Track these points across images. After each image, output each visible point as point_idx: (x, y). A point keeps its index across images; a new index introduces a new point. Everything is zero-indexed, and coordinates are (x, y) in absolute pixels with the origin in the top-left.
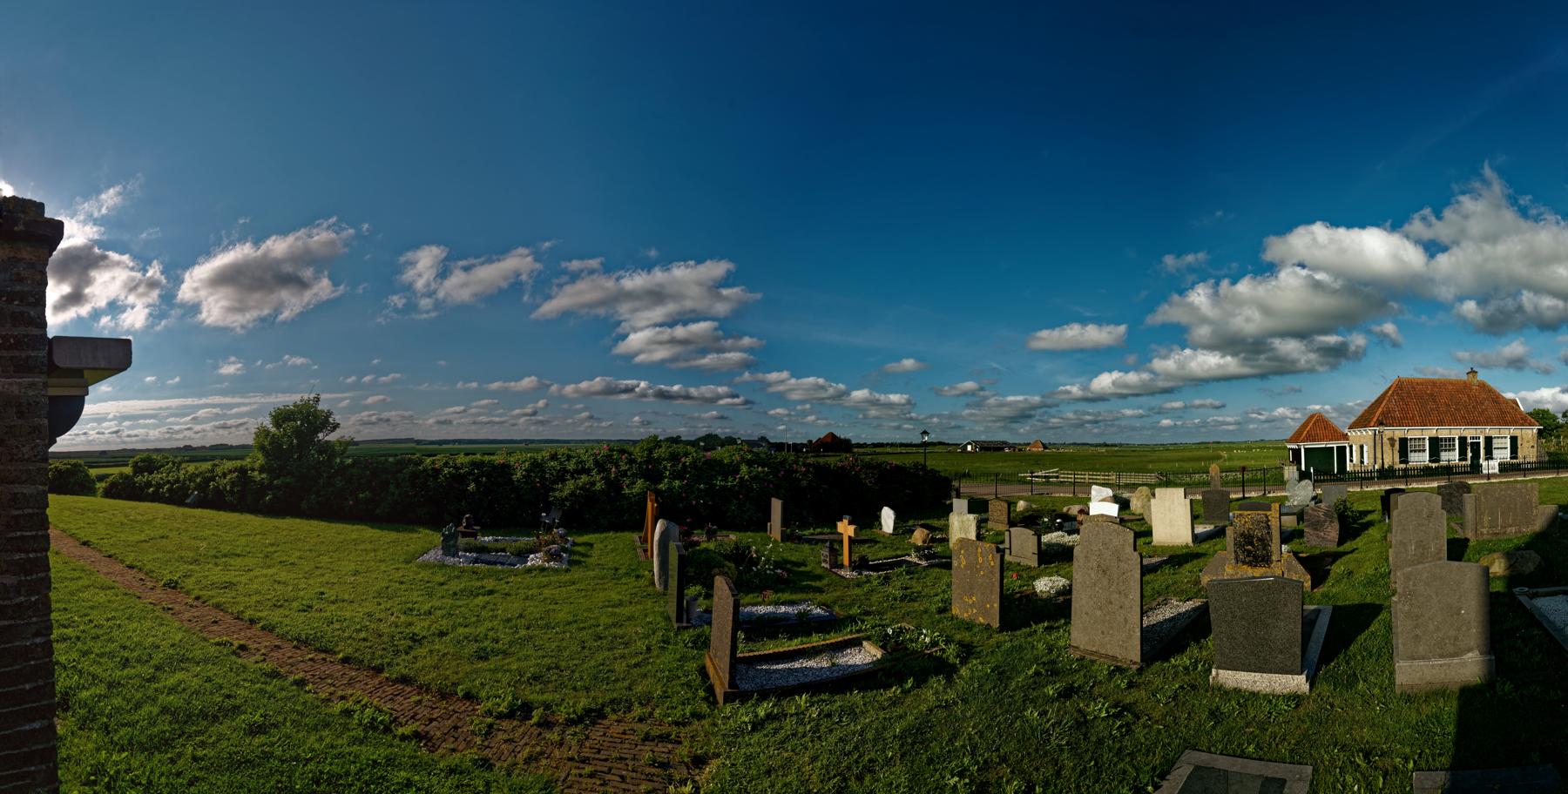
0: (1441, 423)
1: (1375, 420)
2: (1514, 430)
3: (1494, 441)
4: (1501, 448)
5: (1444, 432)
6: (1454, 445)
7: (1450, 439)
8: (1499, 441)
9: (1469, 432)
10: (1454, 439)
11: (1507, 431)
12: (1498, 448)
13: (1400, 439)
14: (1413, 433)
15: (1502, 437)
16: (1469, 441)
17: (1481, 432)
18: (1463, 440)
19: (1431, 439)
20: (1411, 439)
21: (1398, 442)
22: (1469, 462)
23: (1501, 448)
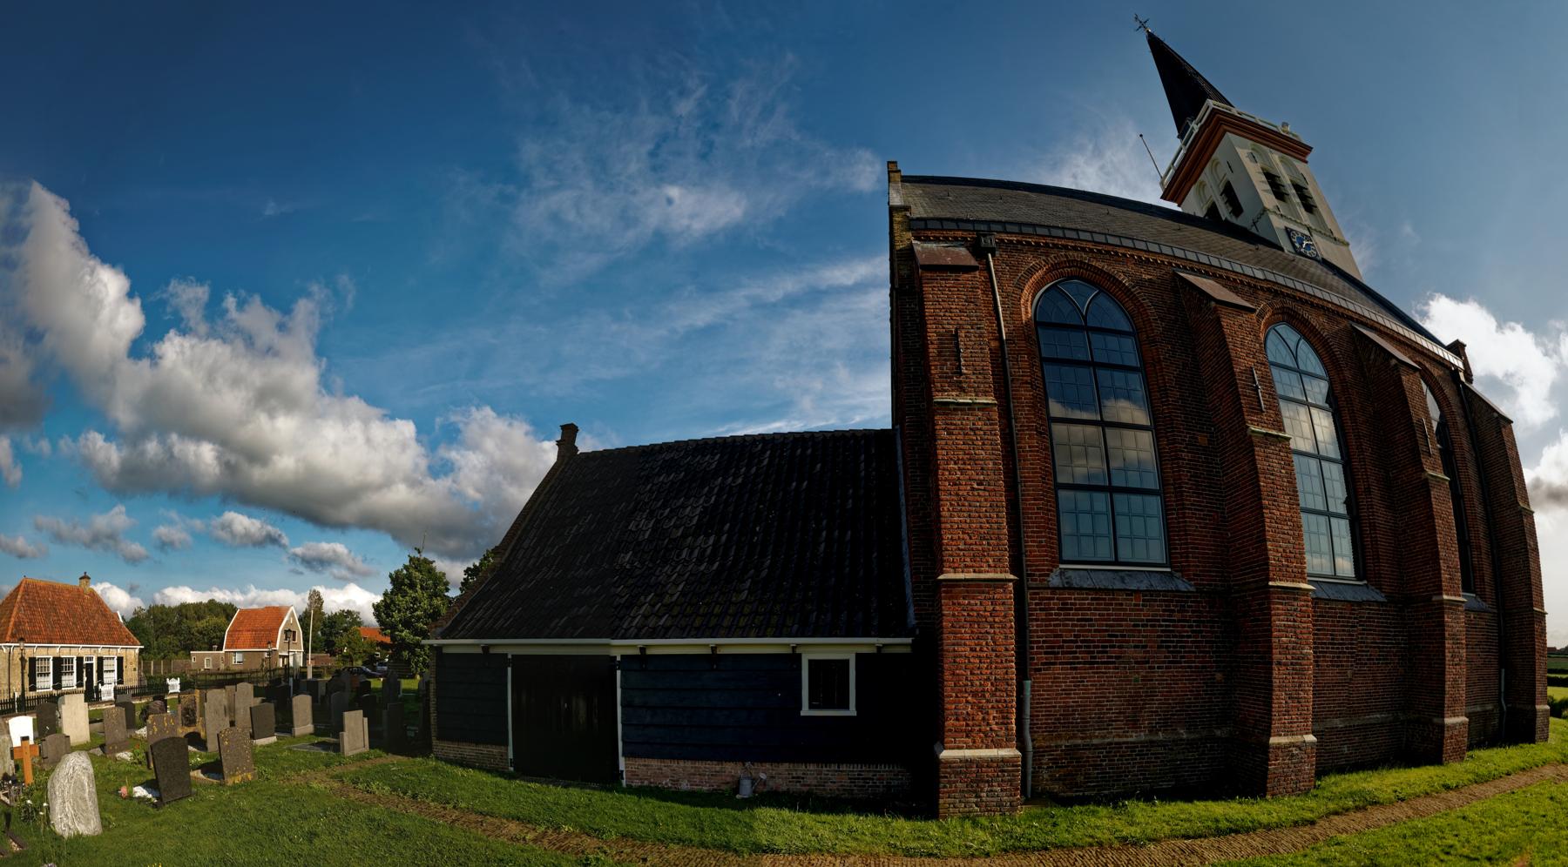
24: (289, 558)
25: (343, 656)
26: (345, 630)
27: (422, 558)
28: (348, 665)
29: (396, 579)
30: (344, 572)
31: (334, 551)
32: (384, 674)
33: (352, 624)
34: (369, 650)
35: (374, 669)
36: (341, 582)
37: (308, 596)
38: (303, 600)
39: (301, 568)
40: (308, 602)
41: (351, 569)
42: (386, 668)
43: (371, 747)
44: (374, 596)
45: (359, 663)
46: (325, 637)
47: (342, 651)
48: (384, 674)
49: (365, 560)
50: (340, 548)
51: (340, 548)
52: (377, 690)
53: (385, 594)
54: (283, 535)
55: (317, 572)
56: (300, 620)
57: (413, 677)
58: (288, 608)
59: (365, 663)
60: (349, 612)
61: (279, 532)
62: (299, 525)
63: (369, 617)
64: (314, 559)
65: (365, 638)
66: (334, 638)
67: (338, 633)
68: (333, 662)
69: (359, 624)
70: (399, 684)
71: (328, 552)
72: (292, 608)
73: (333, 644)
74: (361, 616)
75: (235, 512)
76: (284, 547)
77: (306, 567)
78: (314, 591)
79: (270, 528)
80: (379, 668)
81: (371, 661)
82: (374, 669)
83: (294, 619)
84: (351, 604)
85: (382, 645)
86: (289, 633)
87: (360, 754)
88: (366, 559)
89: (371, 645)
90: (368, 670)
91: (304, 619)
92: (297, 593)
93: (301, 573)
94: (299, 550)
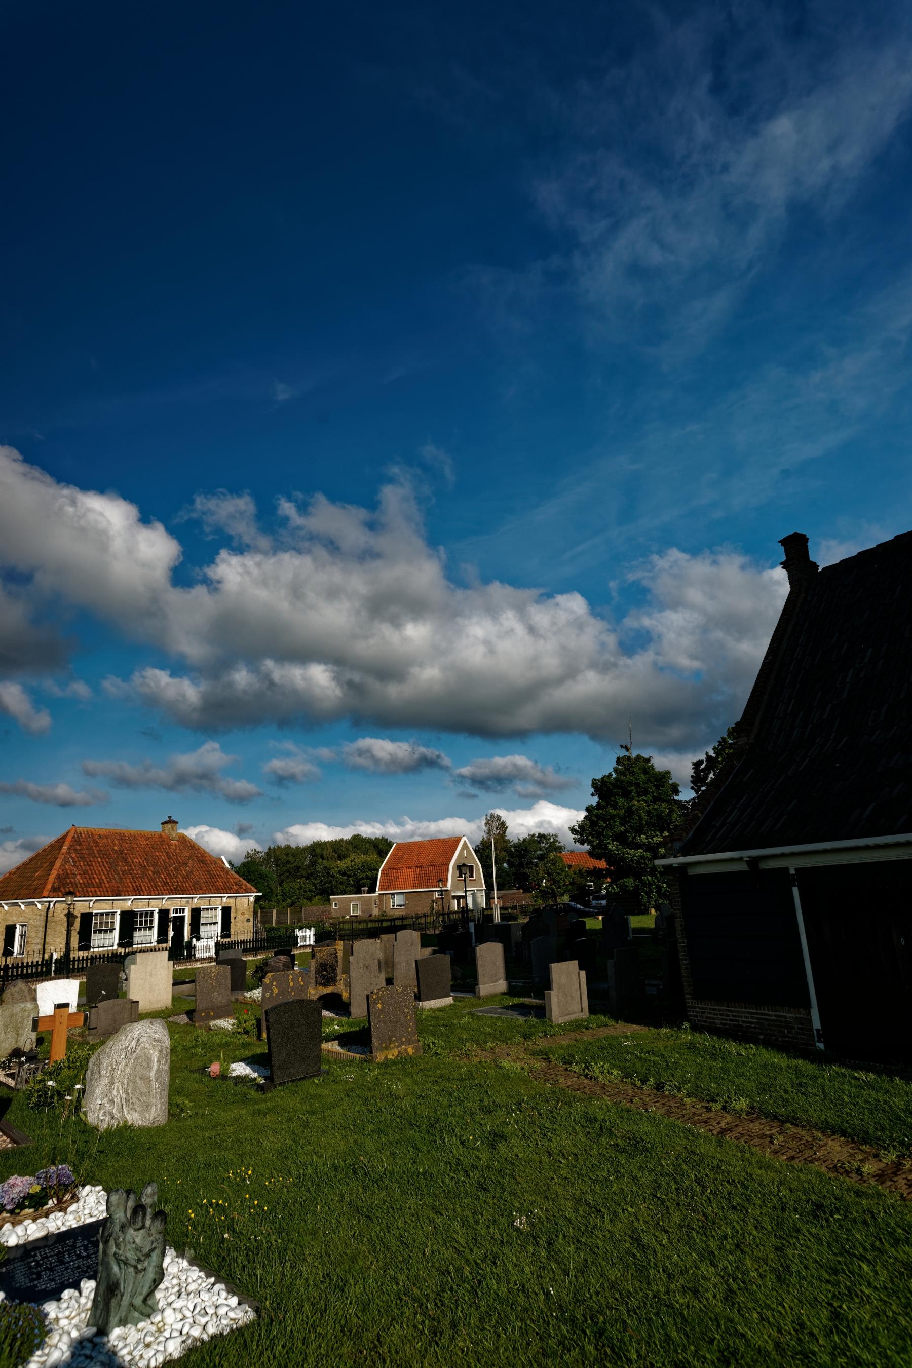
0: (137, 891)
1: (49, 886)
2: (226, 900)
3: (203, 914)
4: (210, 924)
5: (139, 905)
6: (151, 921)
7: (147, 912)
8: (210, 913)
9: (170, 903)
10: (152, 912)
11: (219, 900)
12: (206, 924)
13: (82, 914)
14: (96, 905)
15: (211, 909)
16: (172, 915)
17: (188, 902)
18: (164, 913)
19: (123, 914)
20: (97, 914)
21: (78, 920)
22: (170, 944)
23: (210, 924)
24: (454, 781)
25: (541, 891)
26: (541, 858)
27: (634, 755)
28: (551, 902)
29: (601, 787)
30: (531, 788)
31: (515, 765)
32: (601, 911)
33: (549, 850)
34: (578, 880)
35: (587, 904)
36: (528, 802)
37: (484, 822)
38: (479, 827)
39: (474, 791)
40: (485, 828)
41: (541, 783)
42: (604, 902)
43: (592, 1011)
44: (574, 812)
45: (566, 898)
46: (513, 870)
47: (539, 885)
48: (601, 911)
49: (558, 770)
50: (521, 760)
51: (521, 760)
52: (593, 932)
53: (588, 809)
54: (443, 755)
55: (495, 792)
56: (476, 851)
57: (646, 912)
58: (458, 840)
59: (572, 899)
60: (542, 836)
61: (437, 753)
62: (462, 740)
63: (568, 839)
64: (489, 778)
65: (570, 867)
66: (526, 870)
67: (531, 863)
68: (525, 899)
69: (560, 849)
70: (626, 922)
71: (505, 767)
72: (464, 839)
73: (526, 877)
74: (559, 839)
75: (371, 737)
76: (446, 768)
77: (480, 788)
78: (492, 816)
79: (422, 750)
80: (594, 903)
81: (581, 894)
82: (587, 904)
83: (468, 851)
84: (546, 826)
85: (597, 874)
86: (464, 869)
87: (576, 1021)
88: (560, 769)
89: (581, 873)
90: (579, 906)
91: (482, 850)
92: (470, 820)
93: (475, 796)
94: (466, 770)
